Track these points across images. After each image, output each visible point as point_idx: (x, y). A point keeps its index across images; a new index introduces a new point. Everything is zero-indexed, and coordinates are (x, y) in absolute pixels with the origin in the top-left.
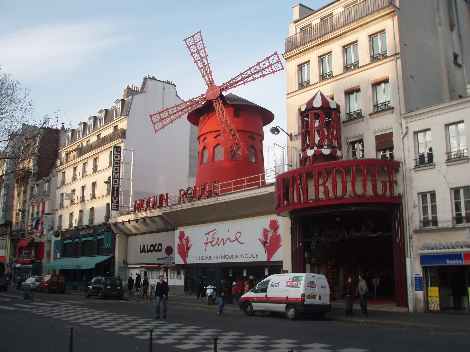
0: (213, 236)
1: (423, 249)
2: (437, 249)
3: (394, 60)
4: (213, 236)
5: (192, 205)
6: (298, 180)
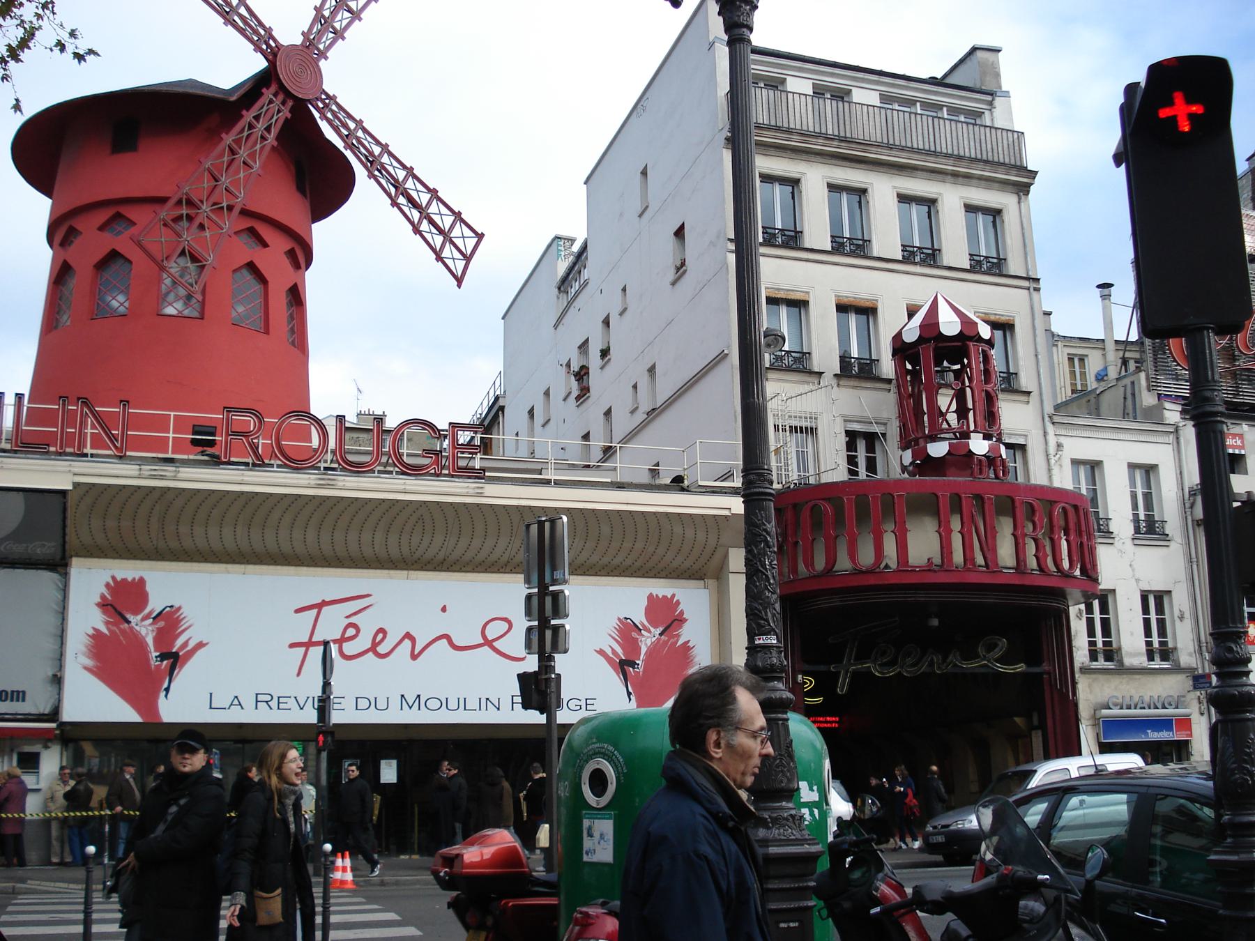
0: (351, 620)
1: (1111, 707)
2: (1135, 708)
3: (1028, 289)
4: (351, 620)
5: (319, 486)
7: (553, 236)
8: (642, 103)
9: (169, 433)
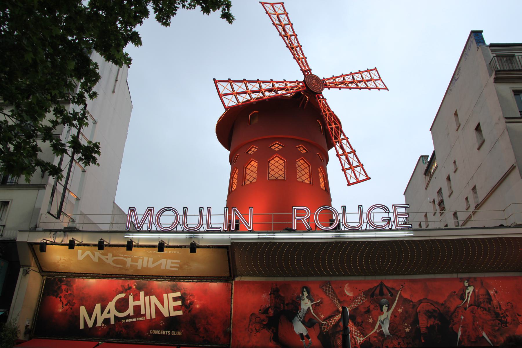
7: (420, 156)
8: (449, 89)
9: (272, 222)
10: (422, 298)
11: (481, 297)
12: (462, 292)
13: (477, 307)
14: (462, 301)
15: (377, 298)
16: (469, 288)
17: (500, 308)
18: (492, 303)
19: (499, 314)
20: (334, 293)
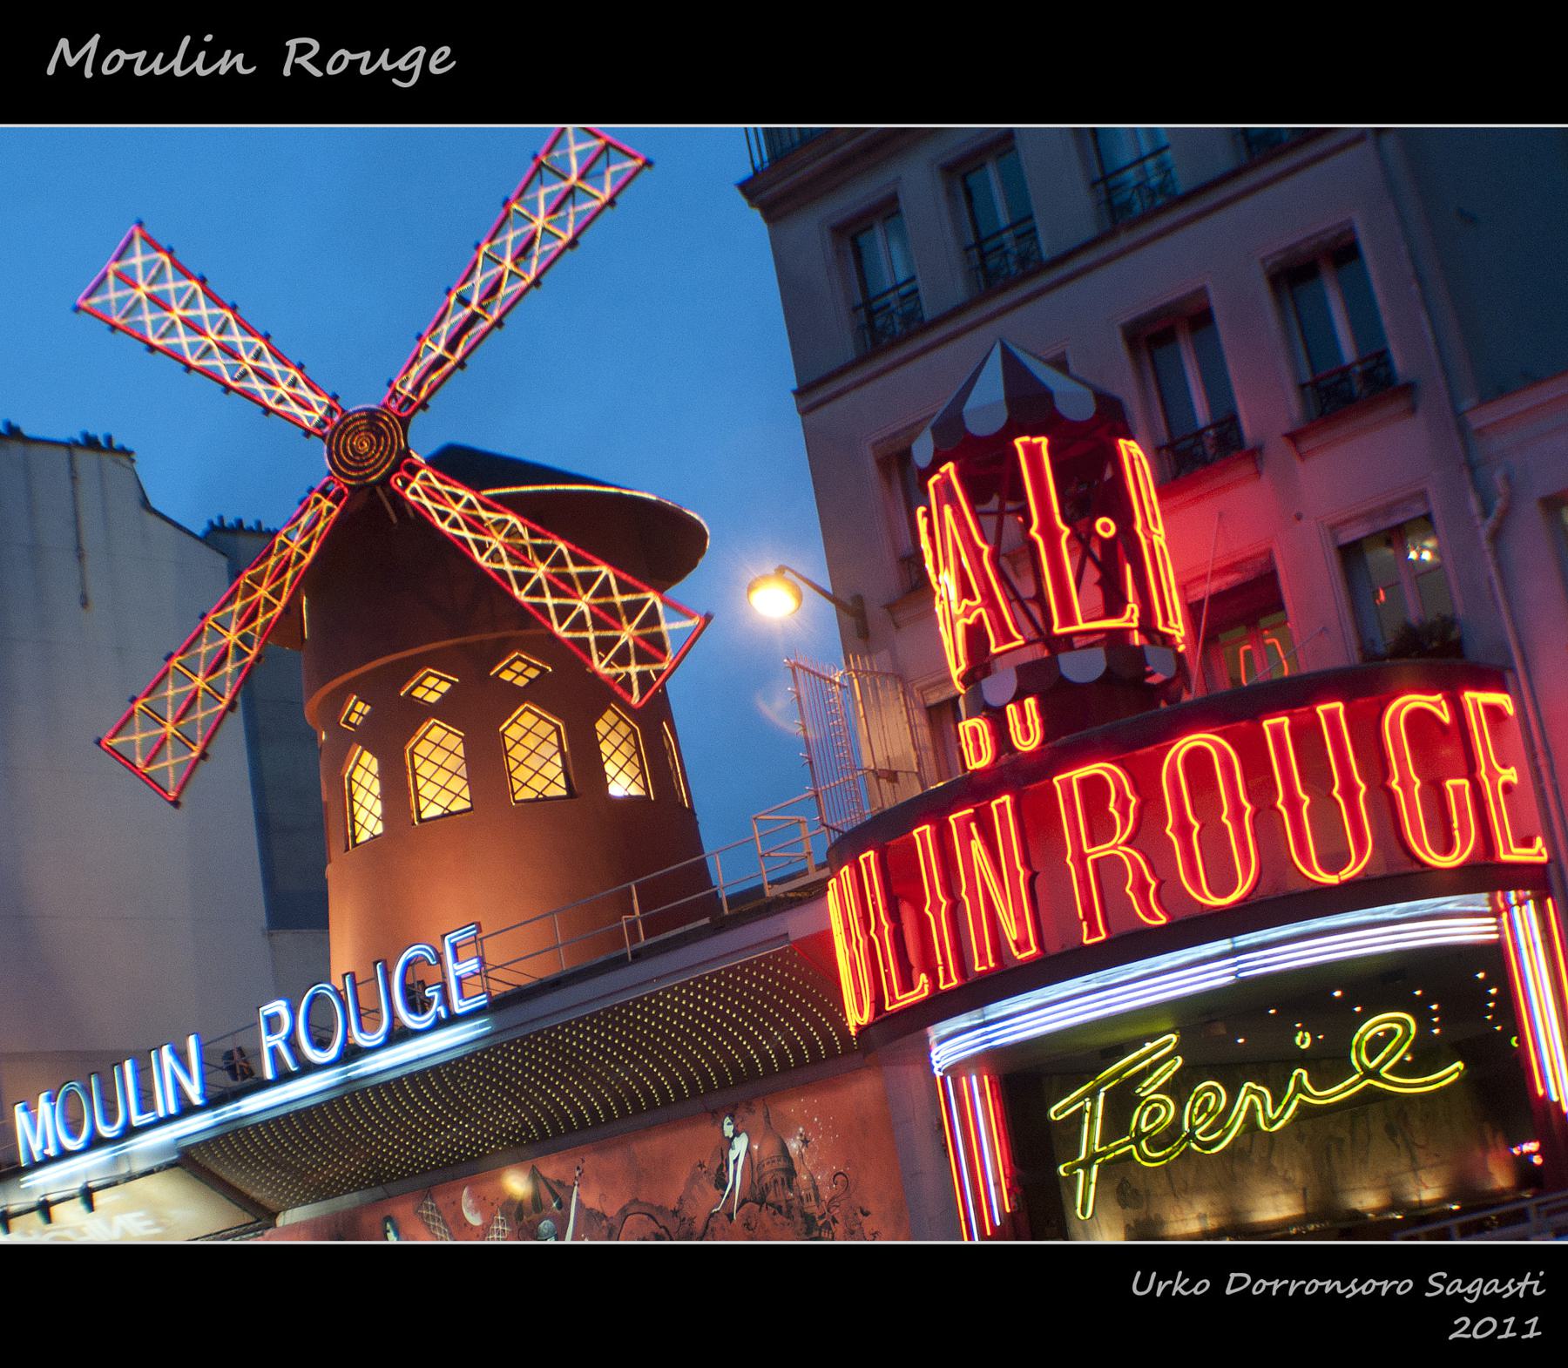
6: (973, 842)
10: (626, 1201)
11: (767, 1168)
12: (716, 1167)
13: (758, 1207)
14: (721, 1191)
15: (529, 1222)
16: (736, 1139)
17: (817, 1197)
18: (795, 1184)
19: (814, 1217)
20: (446, 1225)
